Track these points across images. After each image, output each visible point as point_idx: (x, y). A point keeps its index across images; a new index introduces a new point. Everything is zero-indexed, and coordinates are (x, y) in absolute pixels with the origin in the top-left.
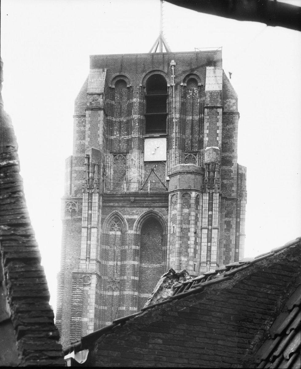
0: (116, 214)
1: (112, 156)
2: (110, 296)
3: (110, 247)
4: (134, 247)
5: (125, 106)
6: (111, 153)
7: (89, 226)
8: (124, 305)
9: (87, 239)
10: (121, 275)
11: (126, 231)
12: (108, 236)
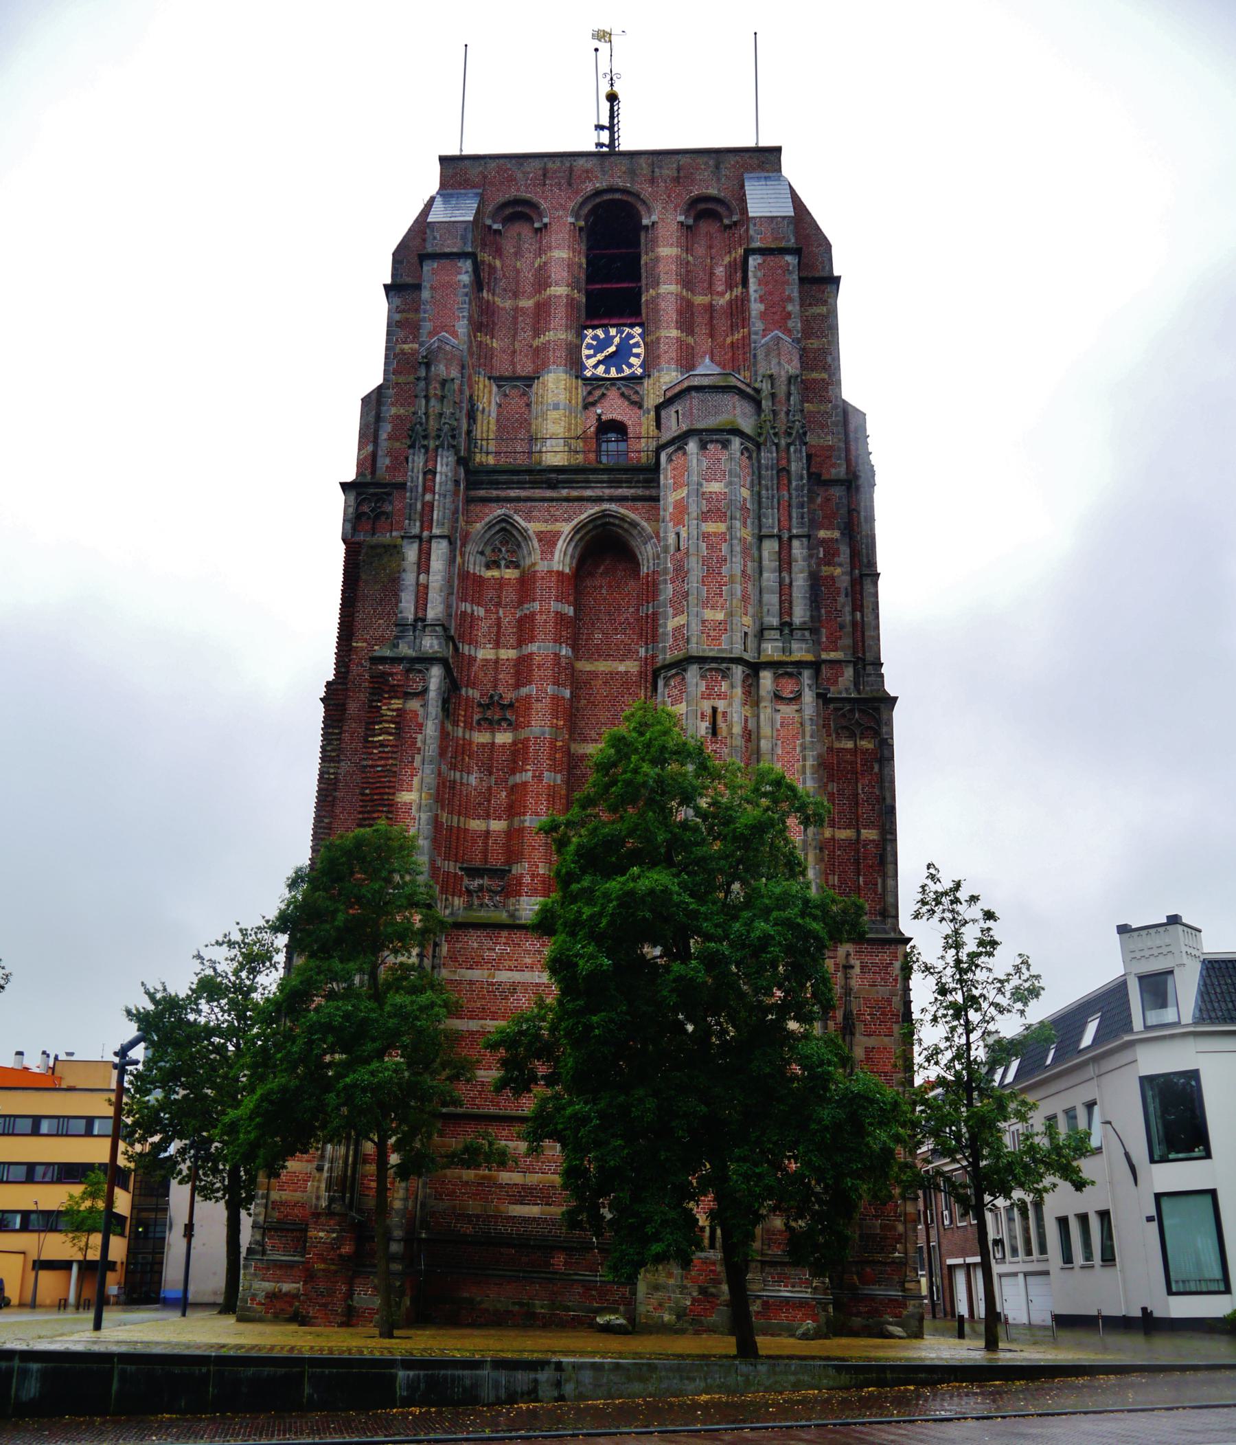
0: (503, 520)
1: (494, 388)
2: (483, 745)
3: (487, 611)
4: (554, 606)
7: (426, 534)
9: (419, 567)
10: (517, 686)
11: (534, 564)
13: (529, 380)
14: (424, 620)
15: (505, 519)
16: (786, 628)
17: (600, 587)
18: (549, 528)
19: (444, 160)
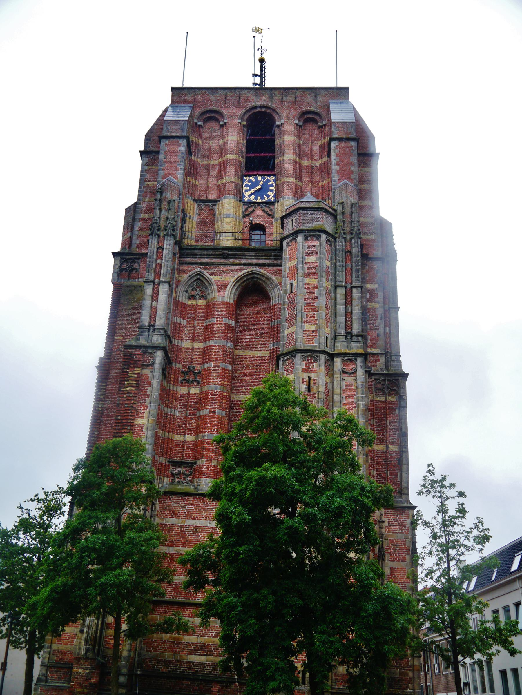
0: (198, 274)
1: (196, 206)
3: (188, 322)
4: (224, 320)
5: (215, 152)
8: (208, 407)
9: (152, 298)
10: (203, 362)
11: (214, 298)
13: (215, 202)
14: (154, 326)
15: (199, 274)
16: (349, 335)
17: (248, 310)
18: (223, 279)
19: (173, 89)
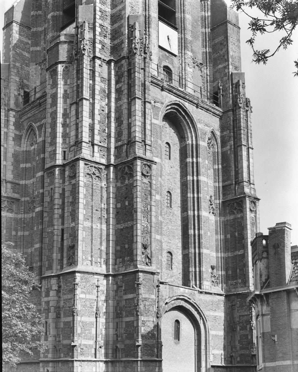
6: (36, 64)
12: (29, 151)
